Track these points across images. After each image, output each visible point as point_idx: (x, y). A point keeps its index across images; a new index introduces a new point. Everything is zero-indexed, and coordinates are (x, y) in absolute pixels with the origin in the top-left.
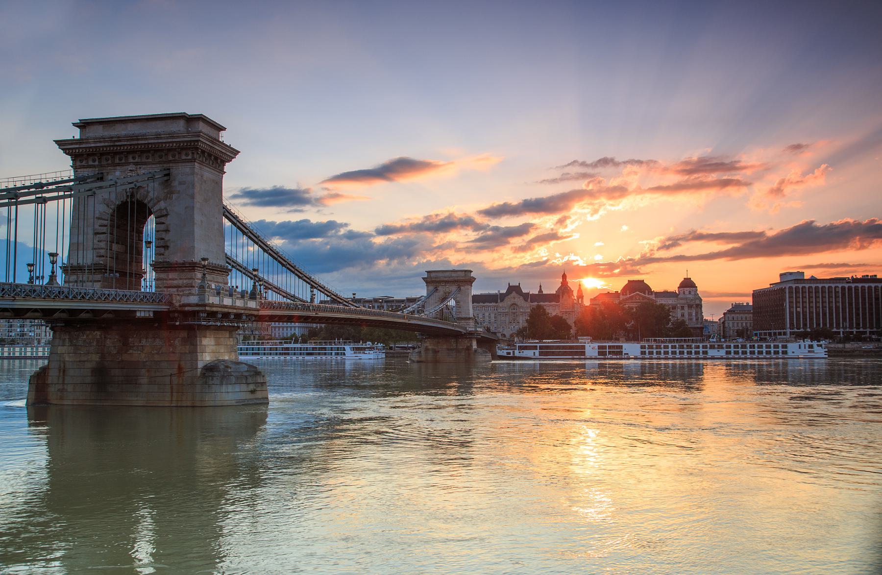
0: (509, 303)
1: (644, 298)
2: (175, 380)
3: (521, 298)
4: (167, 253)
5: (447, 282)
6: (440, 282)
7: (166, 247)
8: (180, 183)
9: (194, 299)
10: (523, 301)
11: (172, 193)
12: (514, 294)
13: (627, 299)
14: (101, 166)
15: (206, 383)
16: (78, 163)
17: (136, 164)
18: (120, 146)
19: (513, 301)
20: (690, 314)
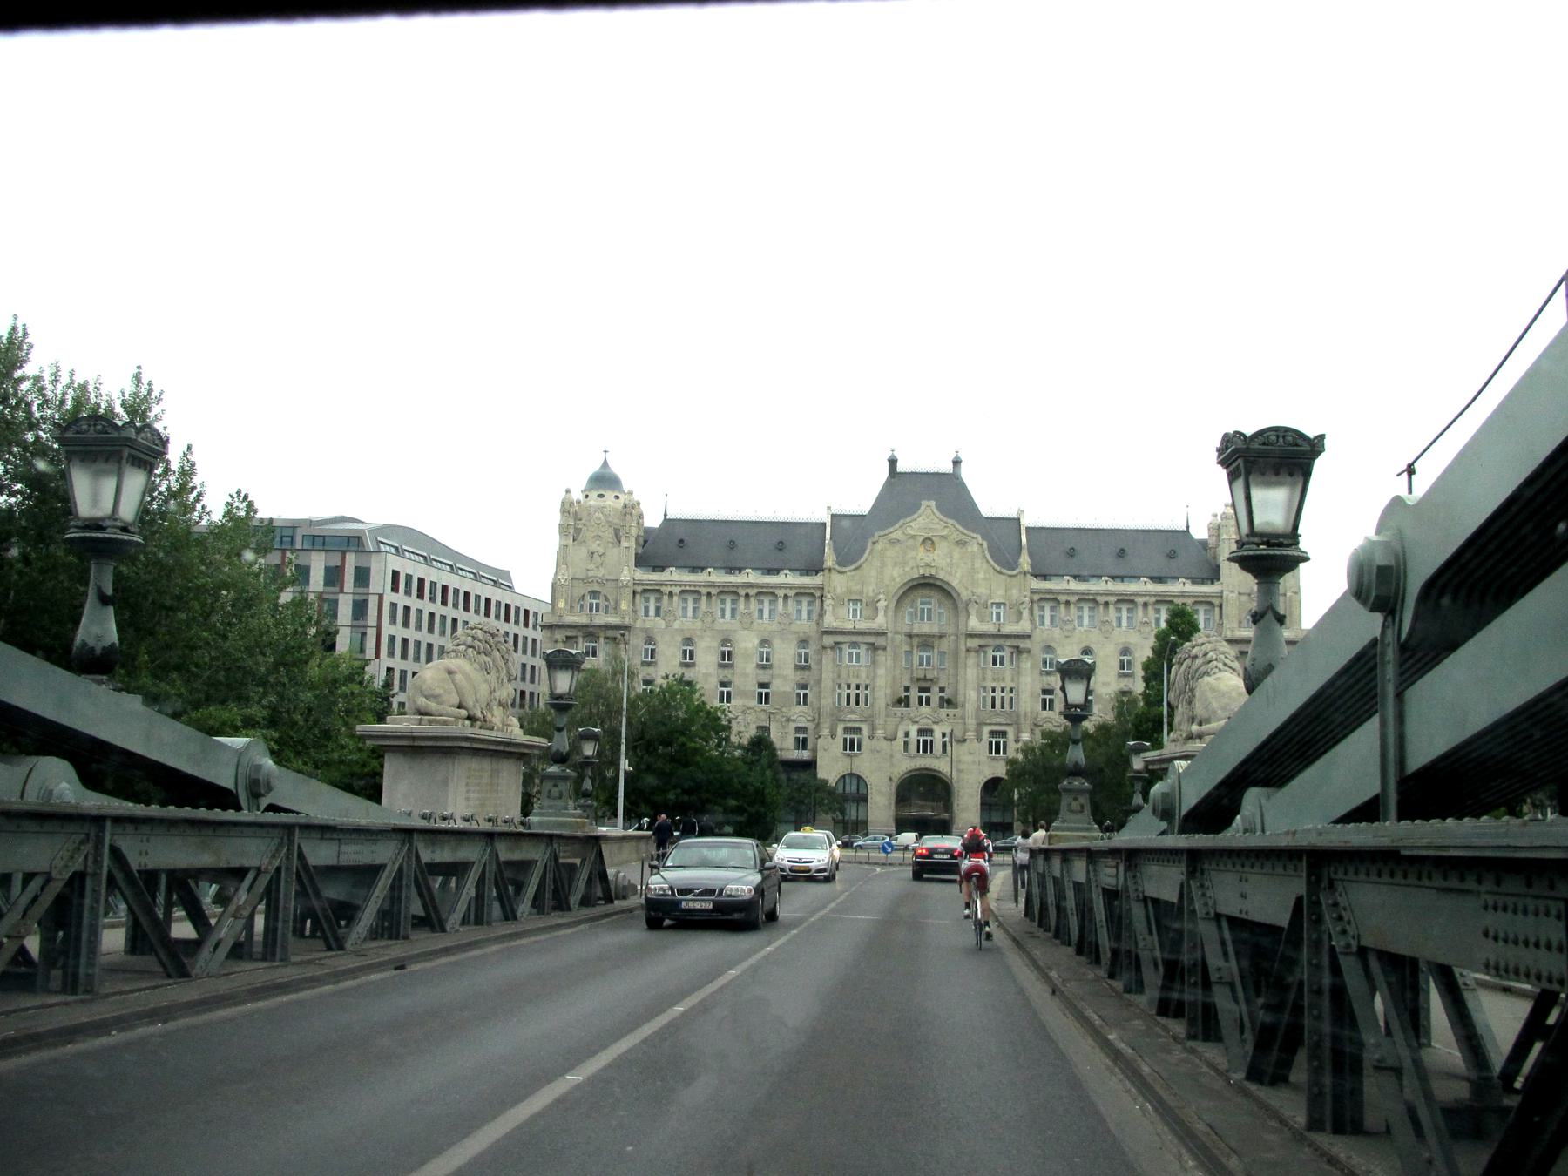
3: (976, 544)
12: (927, 518)
19: (922, 561)
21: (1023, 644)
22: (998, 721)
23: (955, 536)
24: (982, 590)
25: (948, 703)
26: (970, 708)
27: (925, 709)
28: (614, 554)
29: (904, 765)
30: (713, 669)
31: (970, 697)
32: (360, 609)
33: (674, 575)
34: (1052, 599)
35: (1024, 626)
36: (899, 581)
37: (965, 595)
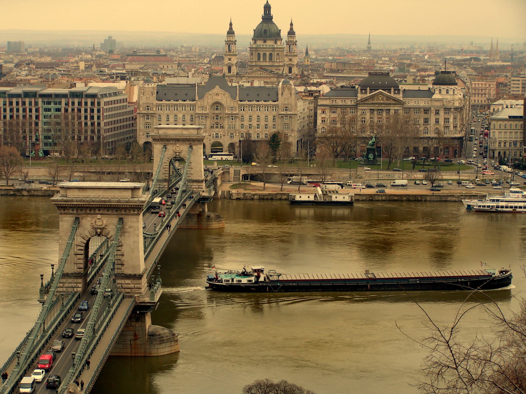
0: (211, 102)
1: (388, 98)
2: (132, 342)
4: (123, 268)
5: (177, 140)
6: (168, 140)
7: (123, 265)
8: (130, 227)
9: (147, 300)
10: (229, 100)
11: (125, 232)
13: (366, 99)
14: (78, 214)
15: (152, 343)
16: (62, 211)
17: (101, 214)
18: (93, 205)
20: (446, 120)
21: (237, 116)
22: (232, 131)
23: (223, 93)
24: (229, 104)
25: (222, 127)
26: (226, 129)
27: (217, 129)
28: (151, 98)
29: (213, 141)
30: (173, 122)
31: (226, 126)
32: (99, 111)
33: (164, 102)
34: (243, 105)
35: (237, 112)
36: (211, 103)
37: (225, 105)
